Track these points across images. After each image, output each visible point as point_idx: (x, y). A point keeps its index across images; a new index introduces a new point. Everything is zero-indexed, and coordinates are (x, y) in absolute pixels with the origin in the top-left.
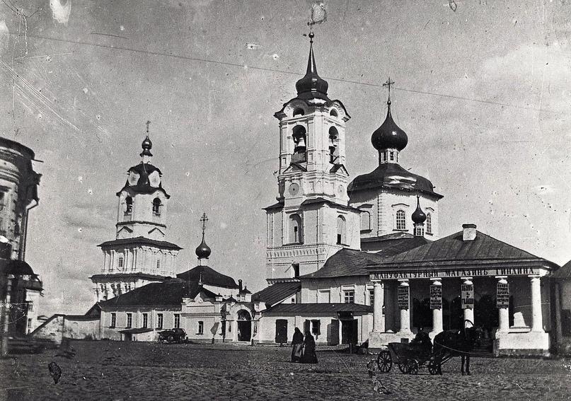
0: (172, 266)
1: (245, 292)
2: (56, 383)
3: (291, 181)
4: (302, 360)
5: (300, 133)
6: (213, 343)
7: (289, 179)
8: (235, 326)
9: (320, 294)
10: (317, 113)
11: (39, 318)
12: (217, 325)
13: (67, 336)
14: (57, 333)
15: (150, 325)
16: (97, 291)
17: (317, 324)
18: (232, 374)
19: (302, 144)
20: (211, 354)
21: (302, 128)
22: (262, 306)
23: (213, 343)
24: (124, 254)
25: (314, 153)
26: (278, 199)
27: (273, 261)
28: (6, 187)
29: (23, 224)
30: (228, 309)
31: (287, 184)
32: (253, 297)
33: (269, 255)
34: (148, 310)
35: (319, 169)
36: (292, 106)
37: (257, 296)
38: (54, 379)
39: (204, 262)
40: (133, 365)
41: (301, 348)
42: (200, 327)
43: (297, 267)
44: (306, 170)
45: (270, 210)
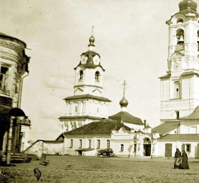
0: (104, 112)
1: (147, 127)
2: (38, 180)
3: (175, 61)
4: (180, 167)
5: (181, 33)
6: (129, 157)
7: (174, 60)
8: (142, 147)
9: (191, 129)
10: (191, 21)
11: (29, 142)
12: (131, 146)
13: (45, 152)
14: (39, 151)
15: (93, 145)
16: (62, 126)
17: (188, 146)
18: (140, 175)
19: (181, 40)
20: (129, 164)
21: (182, 31)
22: (157, 136)
23: (129, 157)
24: (78, 104)
25: (188, 45)
26: (167, 72)
27: (164, 109)
28: (10, 65)
29: (20, 86)
30: (138, 137)
31: (173, 63)
32: (152, 130)
33: (162, 105)
34: (92, 138)
35: (191, 54)
36: (177, 17)
37: (154, 130)
38: (37, 178)
39: (124, 109)
40: (83, 170)
41: (180, 160)
42: (122, 148)
43: (178, 113)
44: (184, 55)
45: (162, 78)
